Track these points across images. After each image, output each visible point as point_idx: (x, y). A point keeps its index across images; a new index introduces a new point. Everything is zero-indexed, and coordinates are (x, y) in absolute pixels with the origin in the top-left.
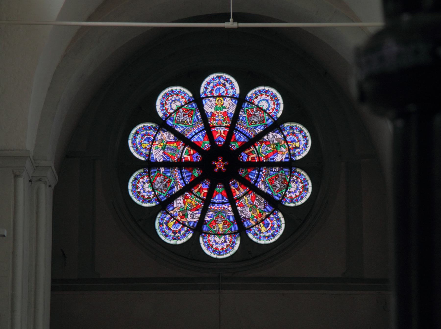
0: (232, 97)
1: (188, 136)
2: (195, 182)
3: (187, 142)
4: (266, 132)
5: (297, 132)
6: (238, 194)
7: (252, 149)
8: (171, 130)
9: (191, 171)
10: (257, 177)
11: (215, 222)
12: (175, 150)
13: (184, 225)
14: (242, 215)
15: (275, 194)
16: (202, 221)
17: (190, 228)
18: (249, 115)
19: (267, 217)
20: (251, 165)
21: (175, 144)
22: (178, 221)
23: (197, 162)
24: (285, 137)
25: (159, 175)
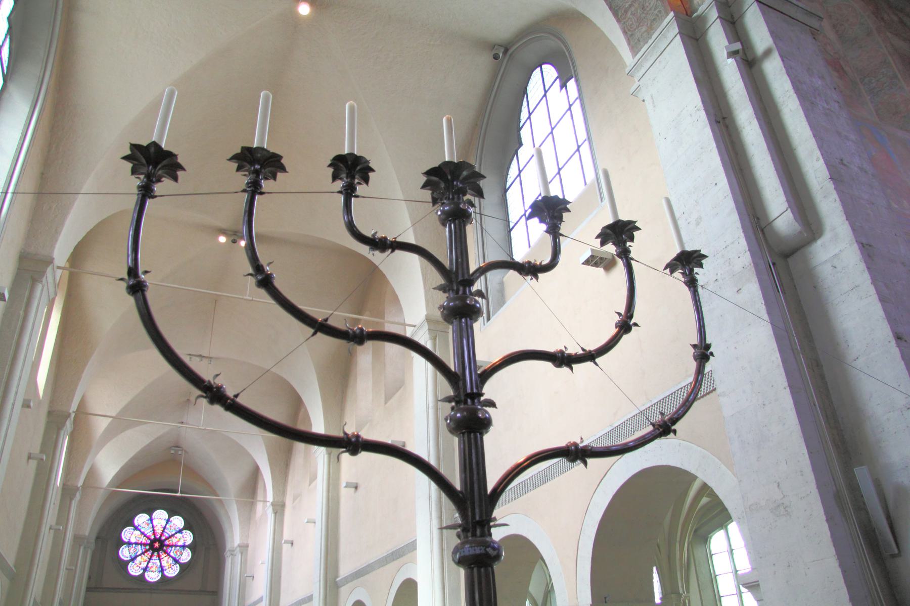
0: (165, 519)
1: (146, 533)
2: (146, 551)
3: (145, 535)
4: (176, 533)
5: (188, 534)
6: (163, 556)
8: (140, 530)
11: (152, 567)
12: (140, 538)
13: (140, 567)
14: (163, 565)
15: (177, 557)
16: (147, 566)
17: (142, 569)
18: (170, 526)
20: (169, 546)
22: (138, 566)
24: (183, 536)
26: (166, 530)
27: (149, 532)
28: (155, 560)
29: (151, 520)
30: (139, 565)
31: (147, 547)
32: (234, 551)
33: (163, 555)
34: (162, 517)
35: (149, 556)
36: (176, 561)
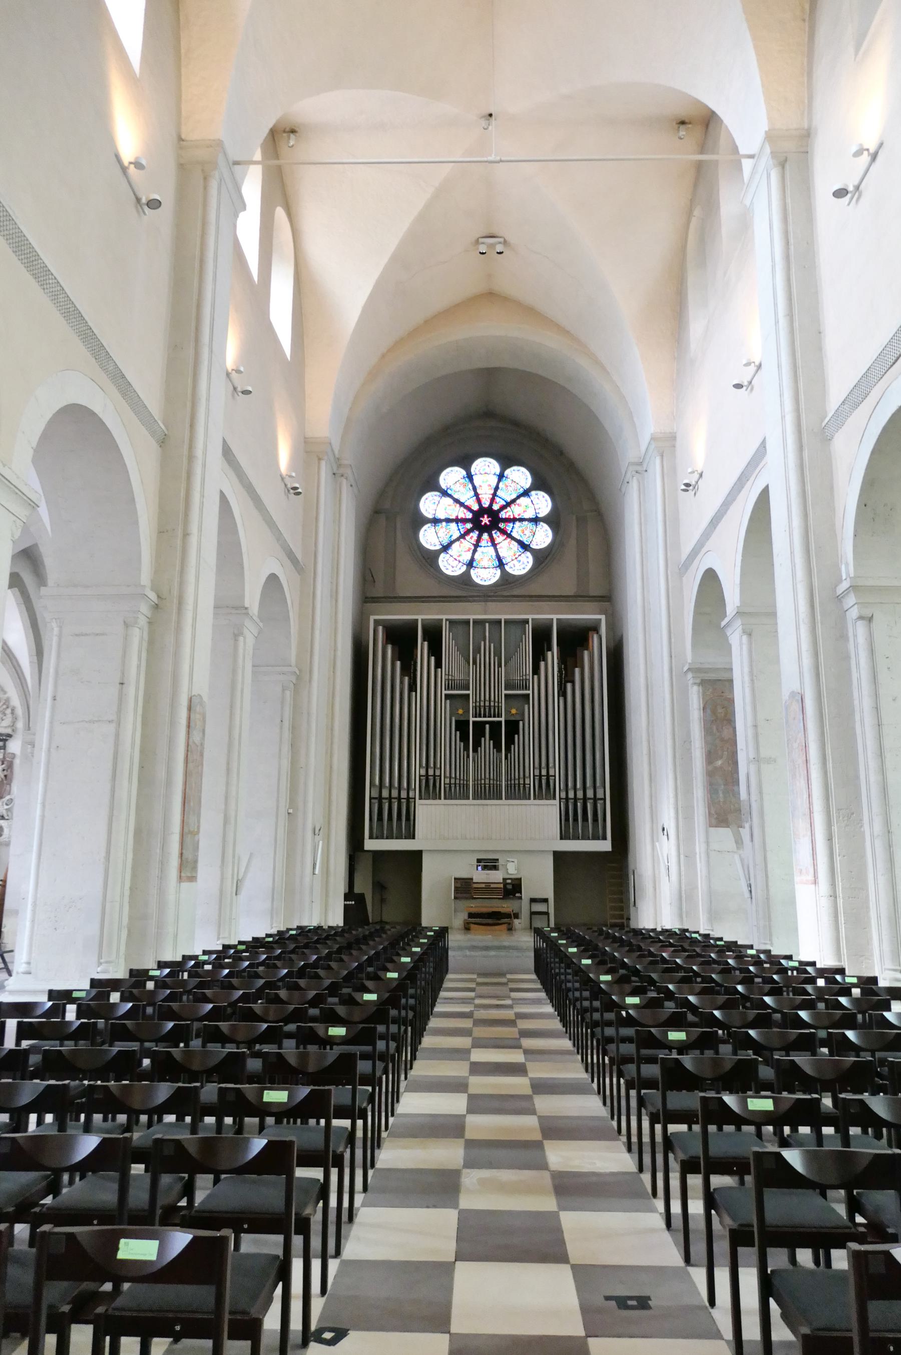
0: (495, 474)
2: (468, 532)
3: (462, 504)
4: (518, 497)
7: (509, 509)
8: (450, 496)
9: (464, 524)
10: (512, 529)
14: (501, 555)
19: (520, 555)
20: (507, 520)
21: (454, 506)
23: (469, 519)
25: (442, 527)
26: (499, 493)
29: (470, 477)
30: (458, 559)
32: (641, 464)
33: (498, 537)
34: (487, 470)
35: (473, 541)
36: (525, 547)
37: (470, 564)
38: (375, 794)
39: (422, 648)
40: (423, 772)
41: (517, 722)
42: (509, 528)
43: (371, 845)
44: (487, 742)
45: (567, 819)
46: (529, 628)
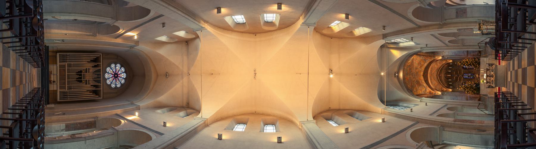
3: (119, 71)
8: (120, 69)
16: (109, 73)
27: (119, 73)
28: (112, 76)
31: (115, 73)
37: (108, 73)
38: (68, 55)
39: (96, 64)
40: (72, 64)
41: (82, 82)
42: (115, 80)
43: (58, 54)
44: (78, 76)
45: (63, 92)
46: (100, 84)
